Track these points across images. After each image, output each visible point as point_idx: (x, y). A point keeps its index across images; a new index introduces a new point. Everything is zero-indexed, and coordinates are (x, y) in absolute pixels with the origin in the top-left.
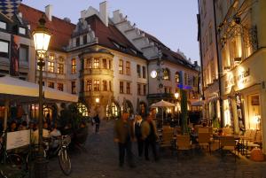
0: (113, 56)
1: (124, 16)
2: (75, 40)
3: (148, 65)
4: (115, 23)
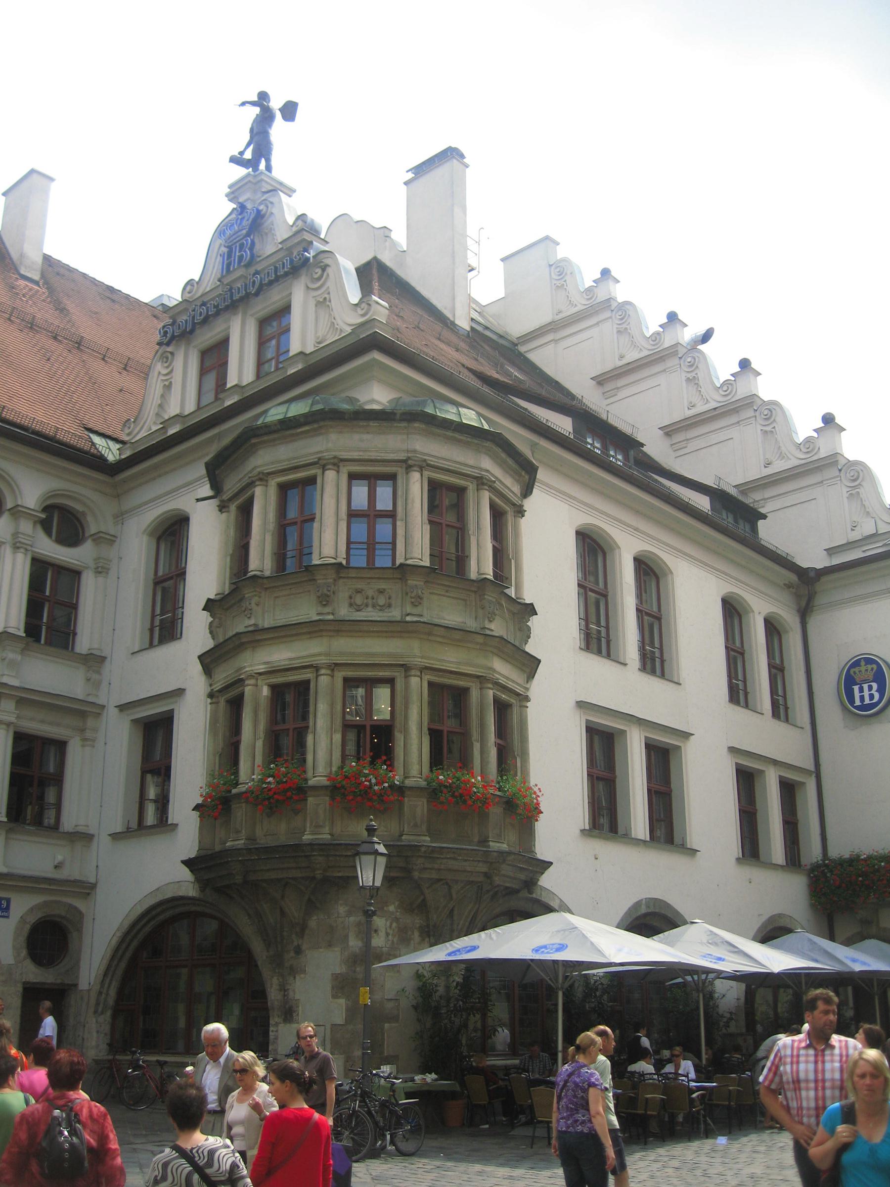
0: (527, 474)
1: (589, 276)
2: (185, 366)
3: (804, 613)
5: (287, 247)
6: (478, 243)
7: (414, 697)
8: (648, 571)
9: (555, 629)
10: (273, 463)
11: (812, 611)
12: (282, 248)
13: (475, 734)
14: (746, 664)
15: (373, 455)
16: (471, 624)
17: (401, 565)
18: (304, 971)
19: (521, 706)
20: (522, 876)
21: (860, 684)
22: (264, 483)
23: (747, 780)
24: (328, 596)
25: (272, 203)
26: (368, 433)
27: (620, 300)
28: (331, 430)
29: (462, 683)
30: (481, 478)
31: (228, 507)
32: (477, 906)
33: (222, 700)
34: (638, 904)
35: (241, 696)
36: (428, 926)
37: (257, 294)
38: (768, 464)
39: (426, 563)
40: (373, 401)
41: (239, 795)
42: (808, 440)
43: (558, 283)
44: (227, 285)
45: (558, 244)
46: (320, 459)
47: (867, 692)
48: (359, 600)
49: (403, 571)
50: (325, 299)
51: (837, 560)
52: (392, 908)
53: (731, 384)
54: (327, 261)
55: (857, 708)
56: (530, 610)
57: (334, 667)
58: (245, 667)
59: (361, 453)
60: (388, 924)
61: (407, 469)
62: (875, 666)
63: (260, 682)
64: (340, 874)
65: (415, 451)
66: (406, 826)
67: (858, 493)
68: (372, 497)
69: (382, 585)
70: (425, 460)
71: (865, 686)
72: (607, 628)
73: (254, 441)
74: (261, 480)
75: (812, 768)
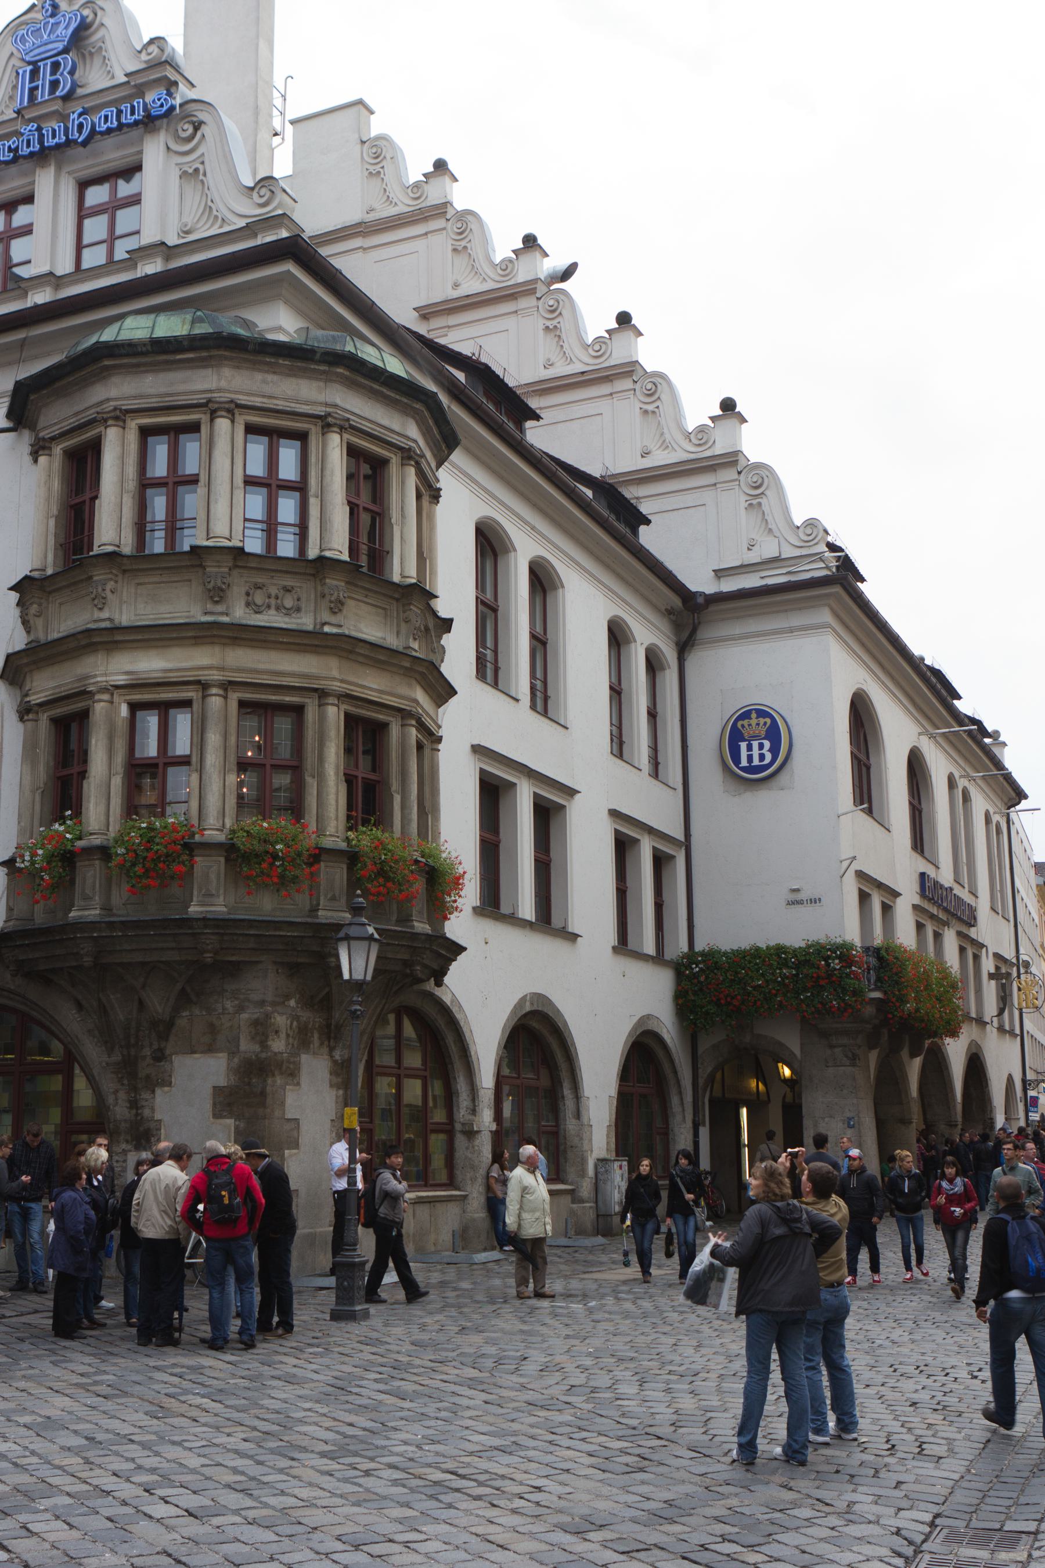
1: (417, 168)
3: (683, 648)
4: (312, 221)
5: (136, 85)
6: (284, 97)
7: (332, 733)
10: (135, 397)
11: (693, 646)
12: (128, 82)
13: (395, 785)
14: (623, 706)
15: (281, 405)
16: (392, 641)
17: (321, 559)
18: (170, 1084)
19: (433, 749)
20: (435, 966)
21: (749, 741)
22: (121, 424)
24: (222, 590)
25: (102, 9)
26: (274, 373)
27: (459, 205)
28: (226, 362)
29: (381, 717)
30: (410, 449)
31: (50, 448)
32: (384, 1001)
33: (44, 718)
34: (523, 999)
35: (84, 716)
36: (329, 1026)
37: (85, 143)
38: (645, 454)
39: (345, 557)
40: (280, 329)
41: (89, 851)
42: (702, 429)
43: (372, 168)
44: (31, 120)
45: (372, 113)
46: (209, 401)
47: (755, 752)
48: (259, 598)
49: (323, 566)
50: (197, 170)
51: (729, 585)
52: (292, 1003)
53: (605, 343)
54: (202, 116)
55: (743, 769)
57: (227, 686)
58: (95, 676)
59: (265, 400)
60: (289, 1022)
61: (323, 428)
62: (768, 721)
63: (116, 698)
64: (234, 959)
65: (336, 406)
66: (322, 898)
67: (760, 504)
68: (272, 460)
69: (289, 582)
70: (348, 420)
71: (755, 744)
72: (495, 651)
73: (107, 363)
74: (117, 418)
75: (682, 838)
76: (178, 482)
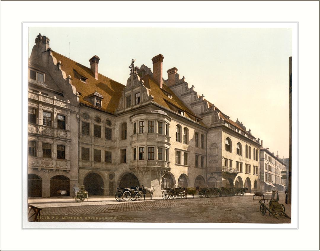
8: (186, 129)
9: (173, 139)
23: (197, 157)
56: (170, 138)
76: (142, 126)
